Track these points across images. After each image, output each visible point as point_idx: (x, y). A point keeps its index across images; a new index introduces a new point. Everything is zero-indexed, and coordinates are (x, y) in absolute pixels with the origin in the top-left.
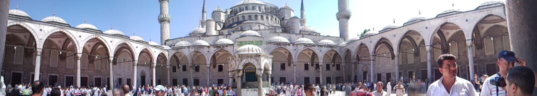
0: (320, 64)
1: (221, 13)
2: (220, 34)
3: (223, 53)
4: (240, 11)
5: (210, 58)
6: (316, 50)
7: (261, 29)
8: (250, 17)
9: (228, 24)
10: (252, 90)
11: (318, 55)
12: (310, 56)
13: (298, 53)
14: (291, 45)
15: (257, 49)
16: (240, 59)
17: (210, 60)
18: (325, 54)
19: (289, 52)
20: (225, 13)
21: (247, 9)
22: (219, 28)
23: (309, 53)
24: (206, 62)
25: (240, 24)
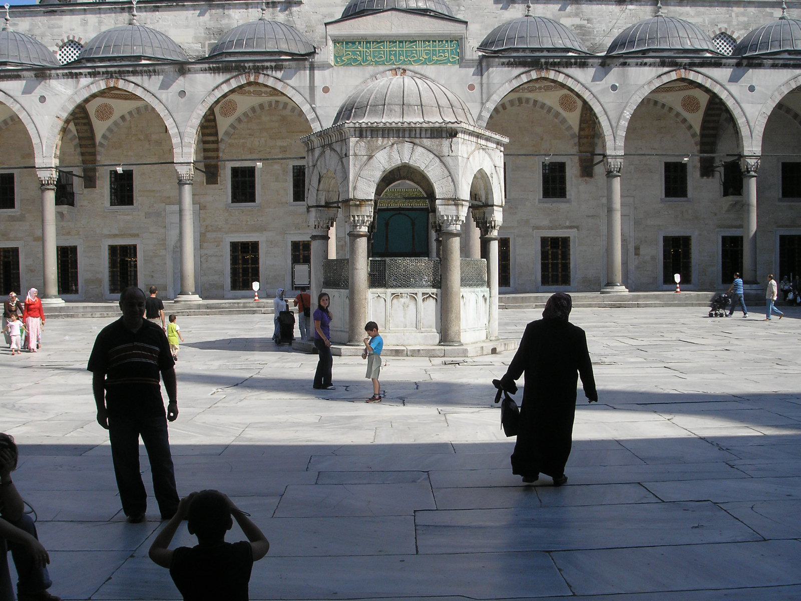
10: (413, 297)
12: (696, 119)
15: (443, 102)
18: (779, 106)
19: (585, 103)
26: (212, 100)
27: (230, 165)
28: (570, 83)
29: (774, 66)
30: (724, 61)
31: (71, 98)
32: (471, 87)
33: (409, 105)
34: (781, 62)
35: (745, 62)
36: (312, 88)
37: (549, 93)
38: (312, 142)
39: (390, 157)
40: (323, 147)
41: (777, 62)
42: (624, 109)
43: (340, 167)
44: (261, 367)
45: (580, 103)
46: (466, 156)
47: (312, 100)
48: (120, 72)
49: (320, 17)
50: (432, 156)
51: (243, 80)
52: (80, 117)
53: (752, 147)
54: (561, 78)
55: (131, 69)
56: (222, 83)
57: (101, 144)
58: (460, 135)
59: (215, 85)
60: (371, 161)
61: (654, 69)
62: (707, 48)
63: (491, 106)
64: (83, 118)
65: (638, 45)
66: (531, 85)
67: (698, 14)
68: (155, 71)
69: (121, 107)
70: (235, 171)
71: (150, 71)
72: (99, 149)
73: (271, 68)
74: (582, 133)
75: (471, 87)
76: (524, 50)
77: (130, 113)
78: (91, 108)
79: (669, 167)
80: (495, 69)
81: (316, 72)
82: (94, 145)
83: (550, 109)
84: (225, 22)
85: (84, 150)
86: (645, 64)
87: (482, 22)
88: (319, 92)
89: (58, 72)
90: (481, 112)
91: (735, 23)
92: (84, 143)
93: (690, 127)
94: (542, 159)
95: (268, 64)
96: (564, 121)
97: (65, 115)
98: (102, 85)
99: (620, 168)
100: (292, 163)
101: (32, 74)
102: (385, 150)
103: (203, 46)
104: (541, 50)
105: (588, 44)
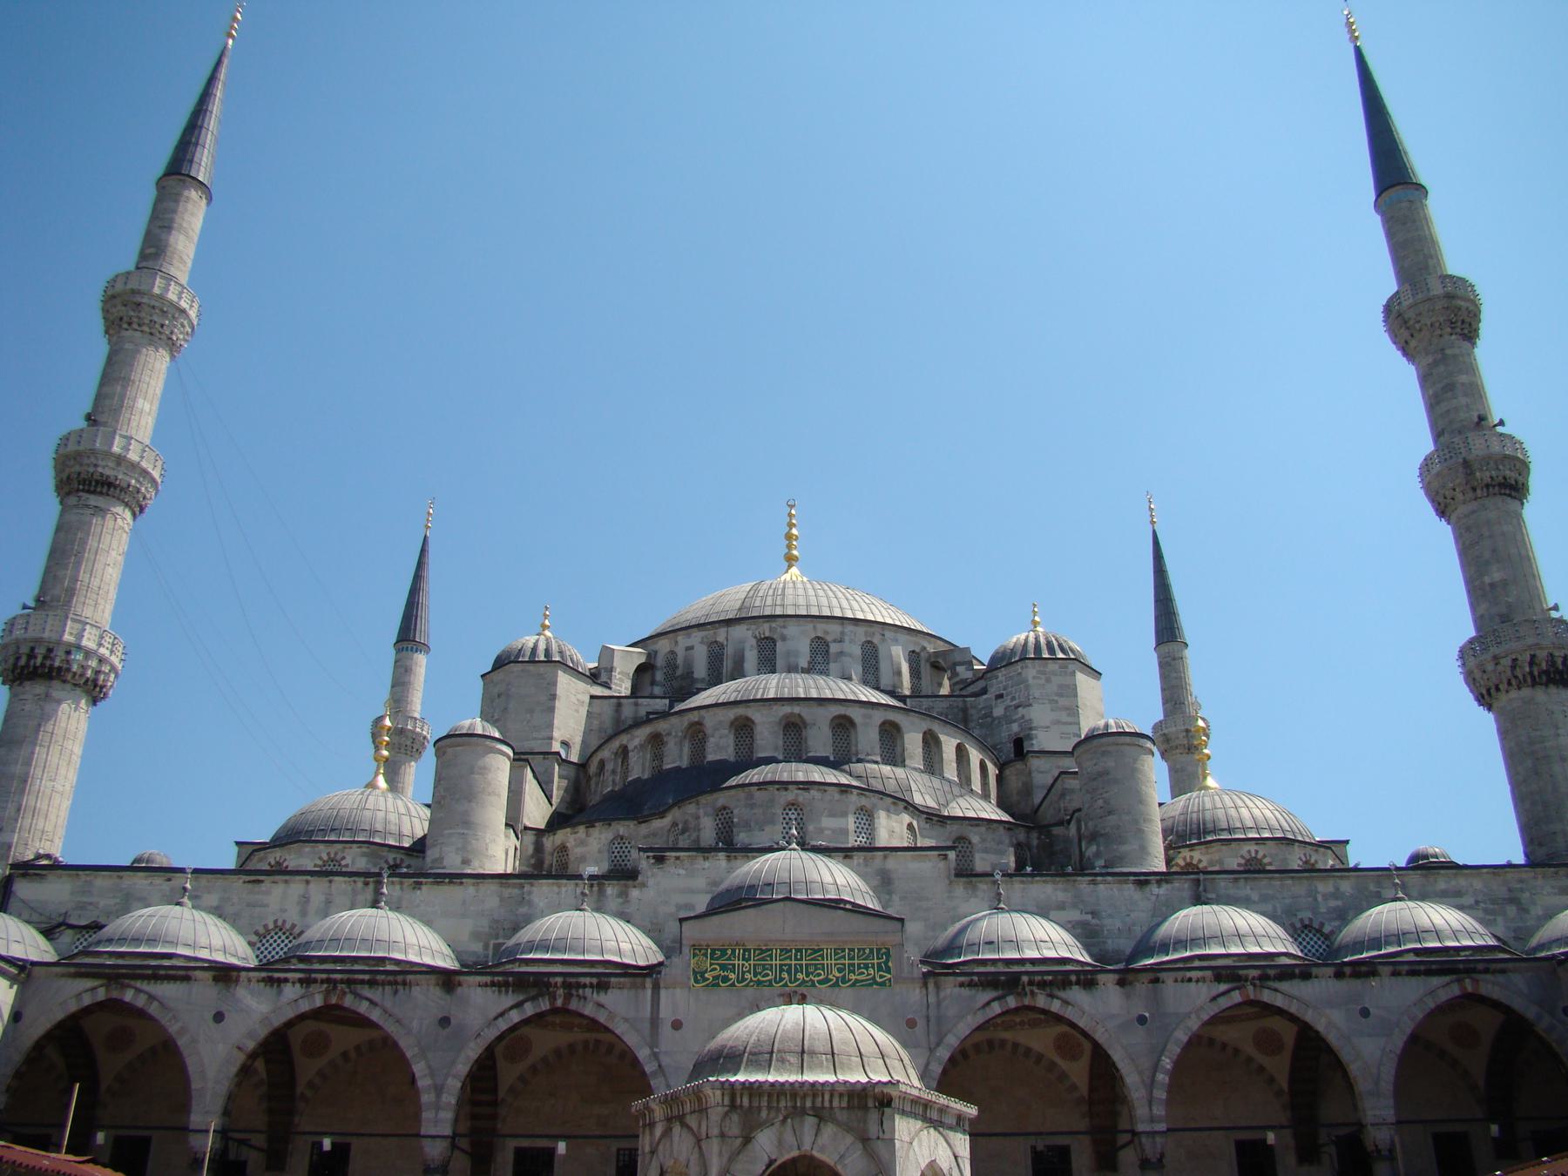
0: (1379, 1136)
1: (563, 679)
2: (543, 865)
3: (562, 1038)
4: (715, 679)
5: (454, 1084)
6: (1322, 1005)
7: (883, 839)
8: (794, 729)
9: (609, 784)
11: (1345, 1055)
12: (1280, 1066)
13: (1174, 1050)
14: (1107, 981)
15: (868, 1048)
16: (734, 1126)
17: (450, 1098)
18: (1414, 1039)
19: (1096, 1046)
20: (594, 677)
21: (768, 664)
22: (537, 811)
23: (1268, 1042)
24: (417, 1117)
25: (716, 788)
26: (491, 1034)
27: (512, 1144)
28: (1069, 1013)
29: (1395, 974)
30: (1315, 971)
31: (265, 1019)
32: (911, 1024)
33: (813, 1053)
34: (1406, 968)
35: (1348, 970)
36: (655, 1021)
38: (651, 1111)
39: (780, 1143)
40: (669, 1120)
41: (1400, 968)
42: (1162, 1053)
43: (694, 1157)
45: (1087, 1046)
46: (907, 1139)
47: (653, 1041)
48: (349, 982)
49: (673, 909)
50: (849, 1139)
51: (544, 1005)
52: (276, 1048)
53: (1378, 1111)
54: (1055, 1006)
55: (367, 977)
56: (511, 1008)
58: (895, 1103)
59: (500, 1010)
60: (750, 1146)
63: (944, 1054)
65: (1175, 950)
66: (1007, 1018)
67: (1265, 898)
68: (404, 983)
69: (343, 1038)
70: (520, 1153)
71: (396, 983)
73: (592, 986)
75: (911, 1024)
76: (994, 961)
77: (358, 1048)
78: (296, 1037)
79: (1241, 1146)
80: (948, 991)
81: (663, 993)
83: (1040, 1058)
84: (523, 910)
86: (1190, 980)
88: (666, 1029)
89: (252, 974)
90: (928, 1064)
93: (1272, 1080)
94: (1032, 1141)
95: (587, 980)
96: (1063, 1076)
97: (251, 1045)
98: (319, 1001)
99: (1162, 1155)
100: (615, 1145)
101: (209, 975)
102: (774, 1129)
103: (486, 947)
104: (1022, 961)
105: (1095, 950)
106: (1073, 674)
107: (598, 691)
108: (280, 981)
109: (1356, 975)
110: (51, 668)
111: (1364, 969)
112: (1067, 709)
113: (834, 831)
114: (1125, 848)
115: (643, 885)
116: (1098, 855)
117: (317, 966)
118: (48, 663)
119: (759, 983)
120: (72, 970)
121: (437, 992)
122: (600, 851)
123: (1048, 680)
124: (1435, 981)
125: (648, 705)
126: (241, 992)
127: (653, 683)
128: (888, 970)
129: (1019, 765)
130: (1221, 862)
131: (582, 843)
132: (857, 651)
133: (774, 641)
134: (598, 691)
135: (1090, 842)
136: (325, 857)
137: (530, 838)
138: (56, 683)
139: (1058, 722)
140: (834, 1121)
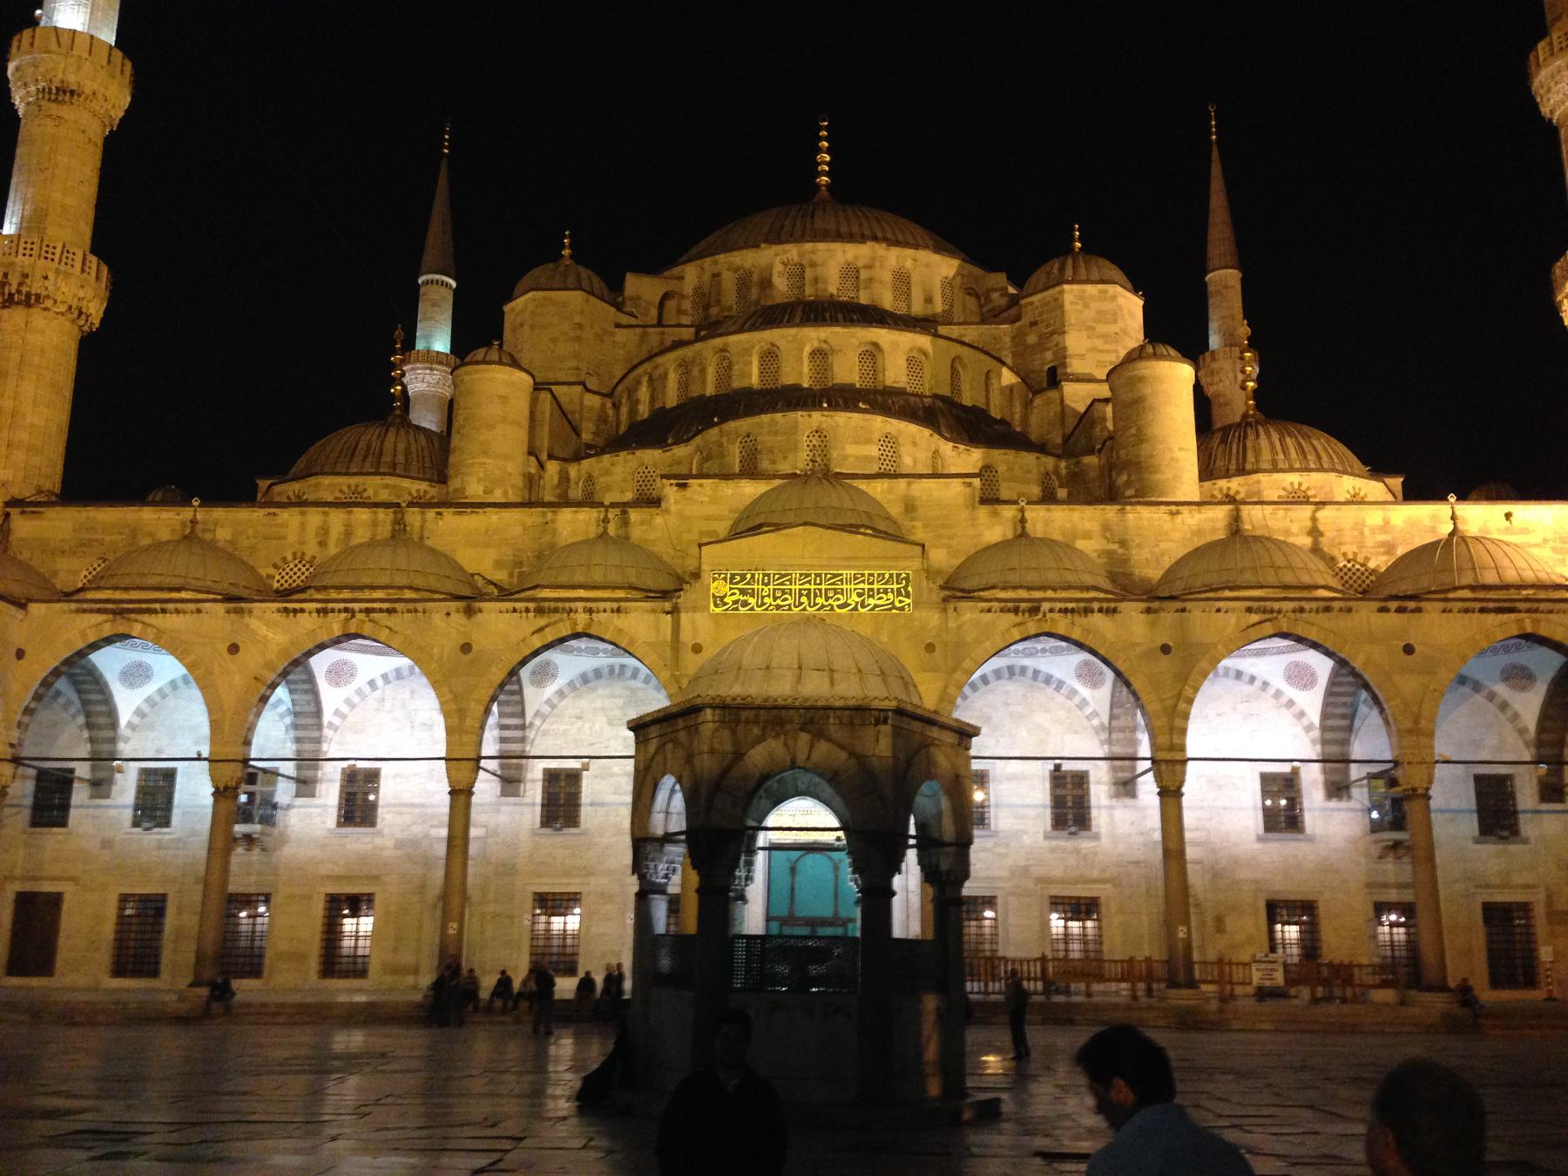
7: (907, 463)
29: (1444, 611)
32: (930, 648)
37: (1058, 659)
41: (1449, 605)
44: (507, 1145)
48: (368, 611)
55: (385, 606)
57: (330, 724)
61: (1232, 619)
62: (1322, 582)
64: (304, 682)
70: (551, 777)
71: (416, 611)
72: (327, 732)
74: (1114, 723)
75: (930, 648)
77: (385, 677)
80: (968, 616)
81: (685, 618)
82: (319, 727)
83: (1060, 684)
85: (301, 734)
86: (1218, 610)
87: (949, 547)
90: (946, 687)
91: (1370, 543)
92: (302, 721)
93: (1302, 714)
103: (511, 575)
106: (1114, 298)
107: (625, 320)
108: (295, 611)
109: (1400, 610)
110: (28, 295)
111: (1412, 605)
112: (1103, 336)
113: (857, 458)
114: (1157, 477)
115: (667, 511)
116: (1128, 484)
117: (334, 595)
118: (24, 289)
119: (778, 607)
120: (73, 606)
121: (458, 619)
122: (624, 480)
123: (1086, 306)
124: (1491, 619)
125: (672, 334)
126: (254, 623)
127: (680, 312)
128: (908, 596)
129: (1053, 394)
130: (1259, 493)
131: (607, 472)
132: (887, 277)
133: (802, 267)
134: (625, 320)
135: (1120, 473)
136: (345, 489)
137: (553, 467)
138: (36, 311)
139: (1094, 349)
140: (829, 739)
